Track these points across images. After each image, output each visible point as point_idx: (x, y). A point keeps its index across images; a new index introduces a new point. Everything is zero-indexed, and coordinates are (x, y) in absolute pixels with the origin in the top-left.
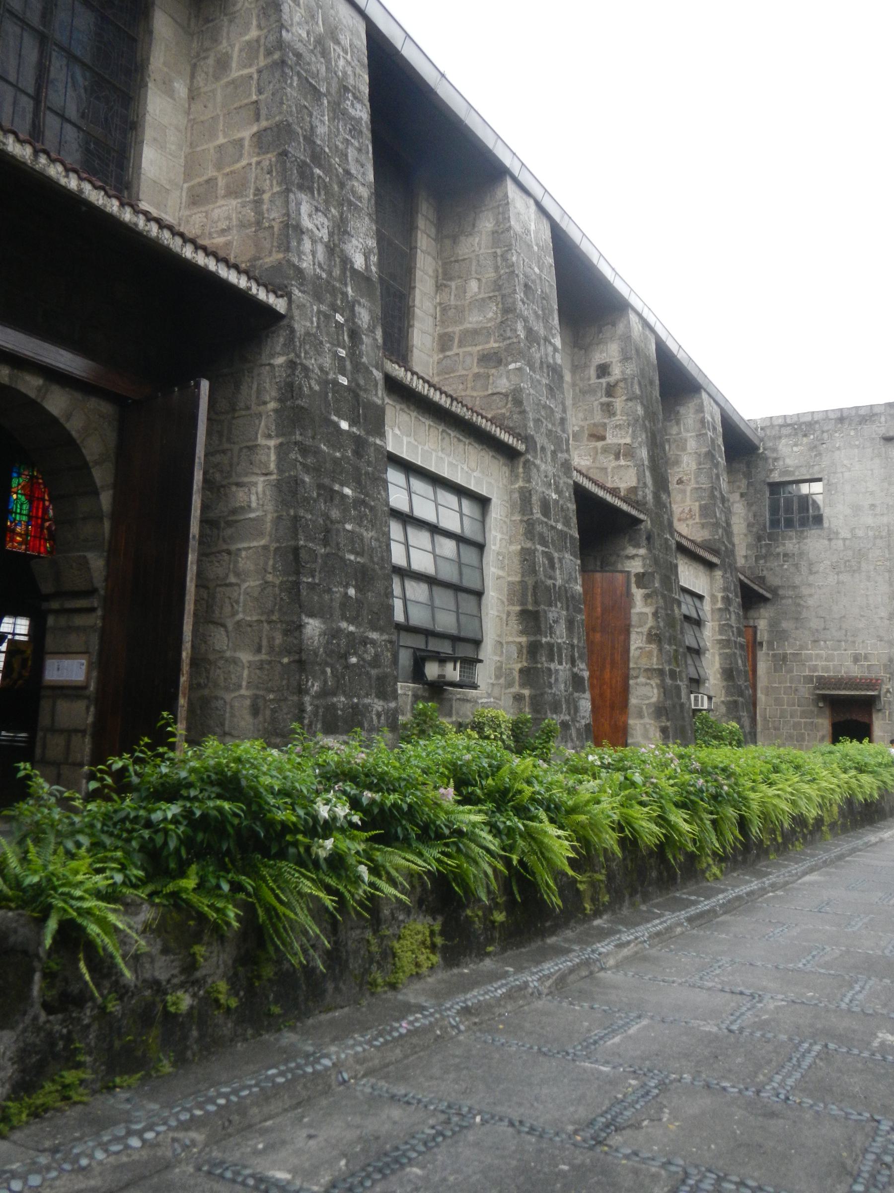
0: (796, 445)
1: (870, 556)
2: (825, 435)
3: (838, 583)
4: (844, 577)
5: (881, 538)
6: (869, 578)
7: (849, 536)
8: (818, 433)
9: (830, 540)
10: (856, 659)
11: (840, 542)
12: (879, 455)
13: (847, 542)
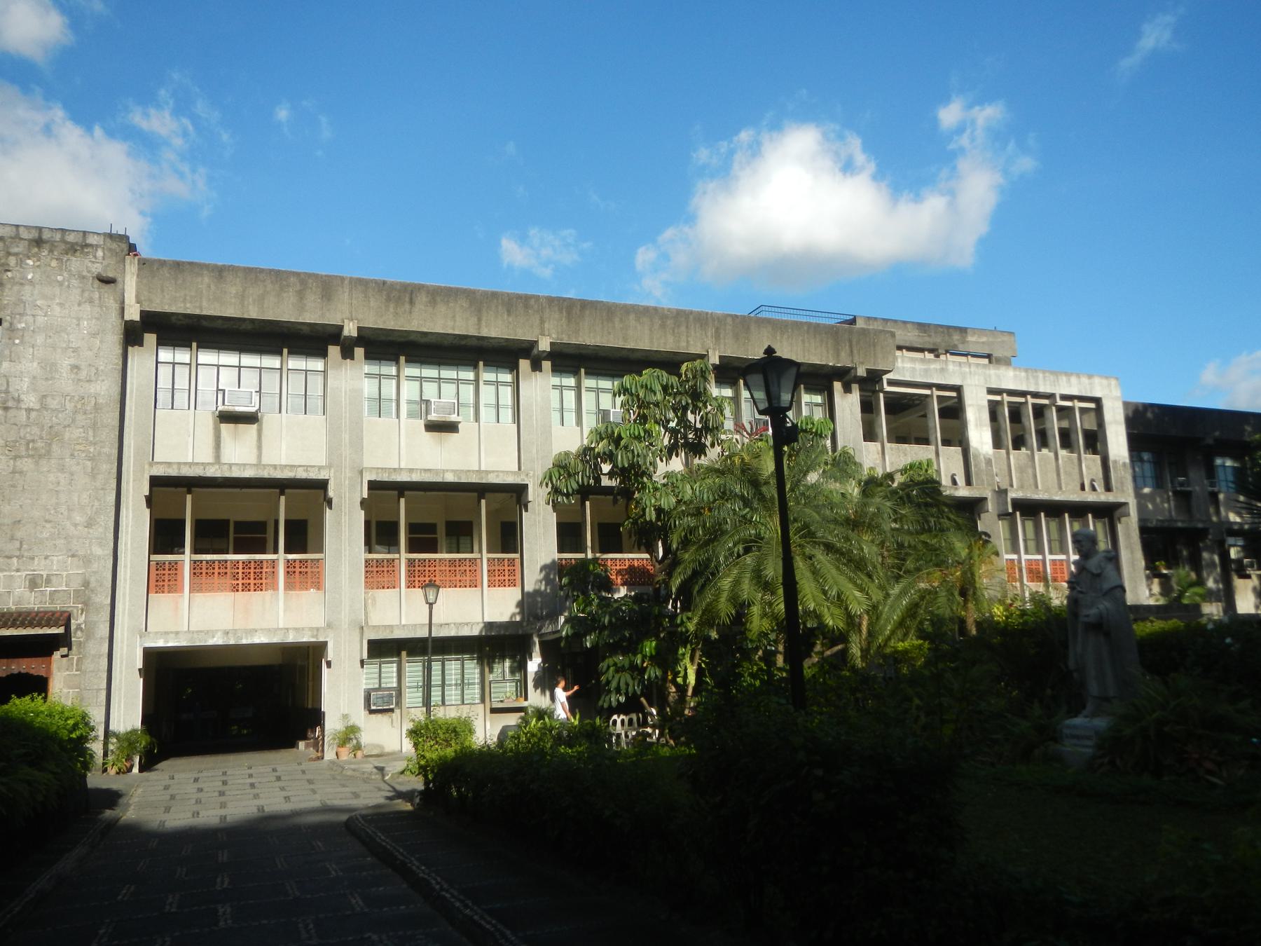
1: (67, 436)
2: (12, 261)
3: (14, 472)
4: (26, 464)
5: (85, 413)
6: (62, 469)
7: (37, 407)
10: (33, 583)
12: (91, 301)
13: (33, 414)
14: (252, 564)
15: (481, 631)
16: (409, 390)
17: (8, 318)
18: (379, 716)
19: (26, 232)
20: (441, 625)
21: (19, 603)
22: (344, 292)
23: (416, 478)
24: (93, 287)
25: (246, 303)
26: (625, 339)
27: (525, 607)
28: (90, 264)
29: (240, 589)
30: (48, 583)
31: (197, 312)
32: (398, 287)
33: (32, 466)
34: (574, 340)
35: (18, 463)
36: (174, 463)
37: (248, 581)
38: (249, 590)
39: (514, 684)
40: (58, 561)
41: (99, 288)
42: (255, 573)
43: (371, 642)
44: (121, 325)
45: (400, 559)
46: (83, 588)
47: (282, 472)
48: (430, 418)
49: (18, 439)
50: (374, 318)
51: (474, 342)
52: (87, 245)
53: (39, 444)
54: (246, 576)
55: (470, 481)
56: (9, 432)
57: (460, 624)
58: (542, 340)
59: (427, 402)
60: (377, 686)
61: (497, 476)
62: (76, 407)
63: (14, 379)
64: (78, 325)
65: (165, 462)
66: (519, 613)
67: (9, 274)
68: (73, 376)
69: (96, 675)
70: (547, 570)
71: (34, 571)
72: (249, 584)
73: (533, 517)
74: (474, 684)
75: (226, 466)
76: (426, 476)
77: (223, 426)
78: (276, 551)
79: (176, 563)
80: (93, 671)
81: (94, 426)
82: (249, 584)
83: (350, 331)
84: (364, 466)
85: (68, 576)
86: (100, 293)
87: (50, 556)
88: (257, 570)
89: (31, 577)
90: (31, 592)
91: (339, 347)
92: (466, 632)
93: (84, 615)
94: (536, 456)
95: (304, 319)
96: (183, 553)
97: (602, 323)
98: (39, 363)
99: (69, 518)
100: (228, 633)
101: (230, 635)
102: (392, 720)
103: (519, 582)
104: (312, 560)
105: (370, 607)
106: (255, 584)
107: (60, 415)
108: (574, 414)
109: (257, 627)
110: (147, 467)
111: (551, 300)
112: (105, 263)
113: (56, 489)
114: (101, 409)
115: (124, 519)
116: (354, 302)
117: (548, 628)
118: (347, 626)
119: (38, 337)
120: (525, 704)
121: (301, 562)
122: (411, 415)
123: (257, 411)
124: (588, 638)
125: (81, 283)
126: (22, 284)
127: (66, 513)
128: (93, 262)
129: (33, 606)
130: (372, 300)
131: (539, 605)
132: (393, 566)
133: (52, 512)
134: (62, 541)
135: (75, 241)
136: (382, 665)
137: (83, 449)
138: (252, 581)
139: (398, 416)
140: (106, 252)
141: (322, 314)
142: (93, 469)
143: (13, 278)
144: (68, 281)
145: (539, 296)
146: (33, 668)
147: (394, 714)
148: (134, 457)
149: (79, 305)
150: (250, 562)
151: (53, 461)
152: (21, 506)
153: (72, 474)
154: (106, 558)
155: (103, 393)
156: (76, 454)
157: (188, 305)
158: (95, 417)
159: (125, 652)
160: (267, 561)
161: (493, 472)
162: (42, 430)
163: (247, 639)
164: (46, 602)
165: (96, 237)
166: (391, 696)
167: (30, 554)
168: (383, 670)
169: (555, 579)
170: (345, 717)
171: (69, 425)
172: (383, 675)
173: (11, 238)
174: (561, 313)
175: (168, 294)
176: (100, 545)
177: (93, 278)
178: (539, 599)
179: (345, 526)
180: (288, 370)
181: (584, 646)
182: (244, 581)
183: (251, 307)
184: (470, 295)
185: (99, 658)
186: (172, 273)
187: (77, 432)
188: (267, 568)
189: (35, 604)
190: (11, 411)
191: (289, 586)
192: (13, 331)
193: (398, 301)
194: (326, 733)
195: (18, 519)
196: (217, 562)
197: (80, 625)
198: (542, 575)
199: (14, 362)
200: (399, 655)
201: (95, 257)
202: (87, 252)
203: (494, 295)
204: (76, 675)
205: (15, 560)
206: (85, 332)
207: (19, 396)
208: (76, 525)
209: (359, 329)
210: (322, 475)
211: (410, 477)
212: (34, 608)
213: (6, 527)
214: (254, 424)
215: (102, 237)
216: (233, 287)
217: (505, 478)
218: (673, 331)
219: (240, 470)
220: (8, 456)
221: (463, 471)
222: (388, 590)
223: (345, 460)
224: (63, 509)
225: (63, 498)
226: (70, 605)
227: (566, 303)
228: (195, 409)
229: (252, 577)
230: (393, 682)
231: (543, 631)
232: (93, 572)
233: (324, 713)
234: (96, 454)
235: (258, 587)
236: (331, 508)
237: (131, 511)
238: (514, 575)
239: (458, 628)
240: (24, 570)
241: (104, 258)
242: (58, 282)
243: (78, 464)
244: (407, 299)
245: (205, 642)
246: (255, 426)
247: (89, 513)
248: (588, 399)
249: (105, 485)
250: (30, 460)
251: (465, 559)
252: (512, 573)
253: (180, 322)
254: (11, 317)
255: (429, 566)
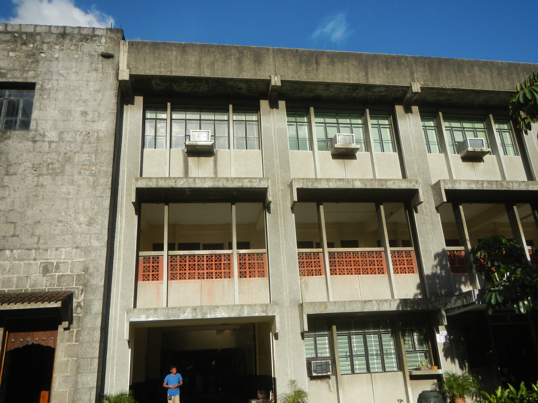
0: (13, 50)
1: (76, 159)
2: (45, 47)
3: (37, 186)
4: (46, 180)
5: (90, 143)
6: (72, 183)
8: (39, 43)
9: (35, 142)
10: (46, 270)
11: (47, 144)
12: (96, 70)
13: (54, 145)
14: (214, 257)
15: (398, 306)
16: (318, 132)
17: (40, 82)
18: (319, 382)
19: (56, 29)
20: (365, 302)
21: (34, 285)
22: (269, 58)
23: (332, 185)
24: (98, 61)
25: (202, 67)
26: (474, 84)
27: (427, 288)
28: (96, 47)
29: (205, 277)
30: (57, 269)
31: (169, 74)
32: (307, 53)
33: (50, 181)
34: (437, 85)
35: (41, 179)
36: (154, 178)
37: (211, 271)
38: (212, 278)
39: (423, 354)
40: (66, 252)
41: (102, 61)
42: (216, 264)
43: (310, 317)
44: (117, 84)
45: (323, 252)
46: (83, 273)
47: (233, 183)
48: (336, 146)
49: (42, 162)
50: (292, 74)
51: (362, 93)
52: (95, 36)
53: (56, 165)
54: (209, 267)
55: (373, 187)
56: (35, 157)
57: (381, 301)
58: (414, 85)
59: (331, 139)
60: (314, 356)
61: (394, 183)
62: (83, 139)
63: (41, 122)
64: (87, 85)
65: (147, 178)
66: (420, 294)
67: (43, 55)
68: (82, 118)
69: (91, 345)
70: (440, 258)
71: (47, 259)
72: (212, 273)
73: (422, 217)
74: (391, 354)
75: (191, 180)
76: (340, 183)
77: (190, 159)
78: (230, 248)
79: (158, 258)
80: (89, 342)
81: (96, 152)
82: (212, 273)
83: (275, 82)
84: (292, 176)
85: (72, 263)
86: (103, 64)
87: (60, 248)
88: (217, 262)
89: (44, 264)
90: (44, 277)
91: (267, 101)
92: (386, 308)
93: (83, 295)
94: (417, 171)
95: (243, 77)
96: (163, 250)
97: (455, 73)
98: (59, 111)
99: (75, 219)
100: (195, 309)
101: (198, 311)
102: (329, 386)
103: (416, 269)
104: (258, 254)
105: (304, 289)
106: (216, 273)
107: (72, 145)
108: (437, 146)
109: (218, 304)
110: (134, 181)
111: (416, 59)
112: (107, 46)
113: (67, 197)
114: (101, 140)
115: (119, 223)
116: (277, 64)
117: (455, 303)
118: (288, 305)
119: (59, 94)
120: (440, 372)
121: (249, 255)
122: (320, 149)
123: (212, 144)
124: (521, 304)
125: (90, 58)
126: (51, 61)
127: (73, 215)
128: (99, 46)
129: (44, 287)
130: (289, 62)
131: (438, 286)
132: (319, 258)
133: (63, 214)
134: (69, 236)
135: (87, 34)
136: (317, 338)
137: (87, 168)
138: (214, 271)
139: (312, 148)
140: (107, 39)
141: (255, 73)
142: (94, 182)
143: (45, 57)
144: (82, 58)
145: (407, 56)
146: (43, 340)
147: (330, 381)
148: (127, 179)
149: (89, 72)
150: (212, 256)
151: (66, 177)
152: (41, 211)
153: (79, 187)
154: (102, 249)
155: (103, 129)
156: (82, 171)
157: (162, 70)
158: (96, 146)
159: (117, 326)
160: (224, 255)
161: (391, 180)
162: (59, 156)
163: (211, 314)
164: (54, 284)
165: (101, 30)
166: (327, 364)
167: (45, 247)
168: (318, 342)
169: (447, 265)
170: (293, 382)
171: (78, 152)
172: (318, 346)
173: (46, 33)
174: (425, 67)
175: (148, 63)
176: (98, 239)
177: (99, 55)
178: (437, 281)
179: (281, 226)
180: (233, 121)
181: (517, 312)
182: (208, 271)
183: (205, 70)
184: (359, 58)
185: (94, 330)
186: (152, 49)
187: (84, 157)
188: (225, 260)
189: (46, 286)
190: (38, 143)
191: (242, 275)
192: (43, 90)
193: (308, 62)
194: (278, 397)
195: (38, 221)
196: (187, 256)
197: (79, 303)
198: (436, 262)
199: (43, 110)
200: (329, 329)
201: (100, 43)
202: (95, 40)
203: (375, 56)
204: (75, 345)
205: (33, 252)
206: (92, 89)
207: (44, 133)
208: (80, 224)
209: (282, 81)
210: (263, 185)
211: (328, 185)
212: (45, 289)
213: (28, 226)
214: (211, 157)
215: (105, 31)
216: (193, 58)
217: (400, 184)
218: (508, 78)
219: (202, 182)
220: (33, 174)
221: (367, 179)
222: (316, 277)
223: (278, 178)
224: (71, 212)
225: (71, 203)
226: (72, 286)
227: (426, 61)
228: (170, 148)
229: (214, 268)
230: (326, 353)
231: (448, 307)
232: (93, 260)
233: (275, 378)
234: (97, 171)
235: (219, 275)
236: (269, 212)
237: (124, 217)
238: (412, 264)
239: (379, 305)
240: (40, 259)
241: (106, 43)
242: (75, 58)
243: (84, 179)
244: (314, 61)
245: (178, 316)
246: (212, 159)
247: (90, 214)
248: (446, 134)
249: (103, 193)
250: (49, 177)
251: (373, 252)
252: (410, 262)
253: (160, 87)
254: (42, 81)
255: (346, 258)
